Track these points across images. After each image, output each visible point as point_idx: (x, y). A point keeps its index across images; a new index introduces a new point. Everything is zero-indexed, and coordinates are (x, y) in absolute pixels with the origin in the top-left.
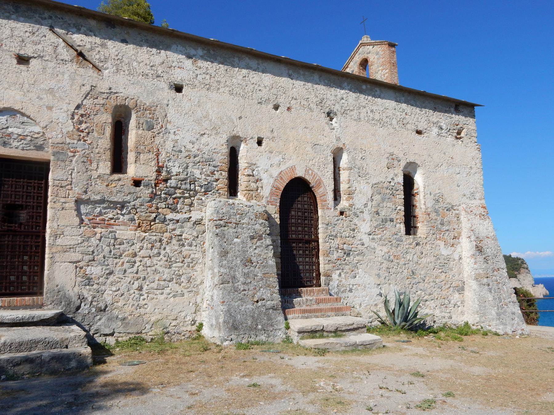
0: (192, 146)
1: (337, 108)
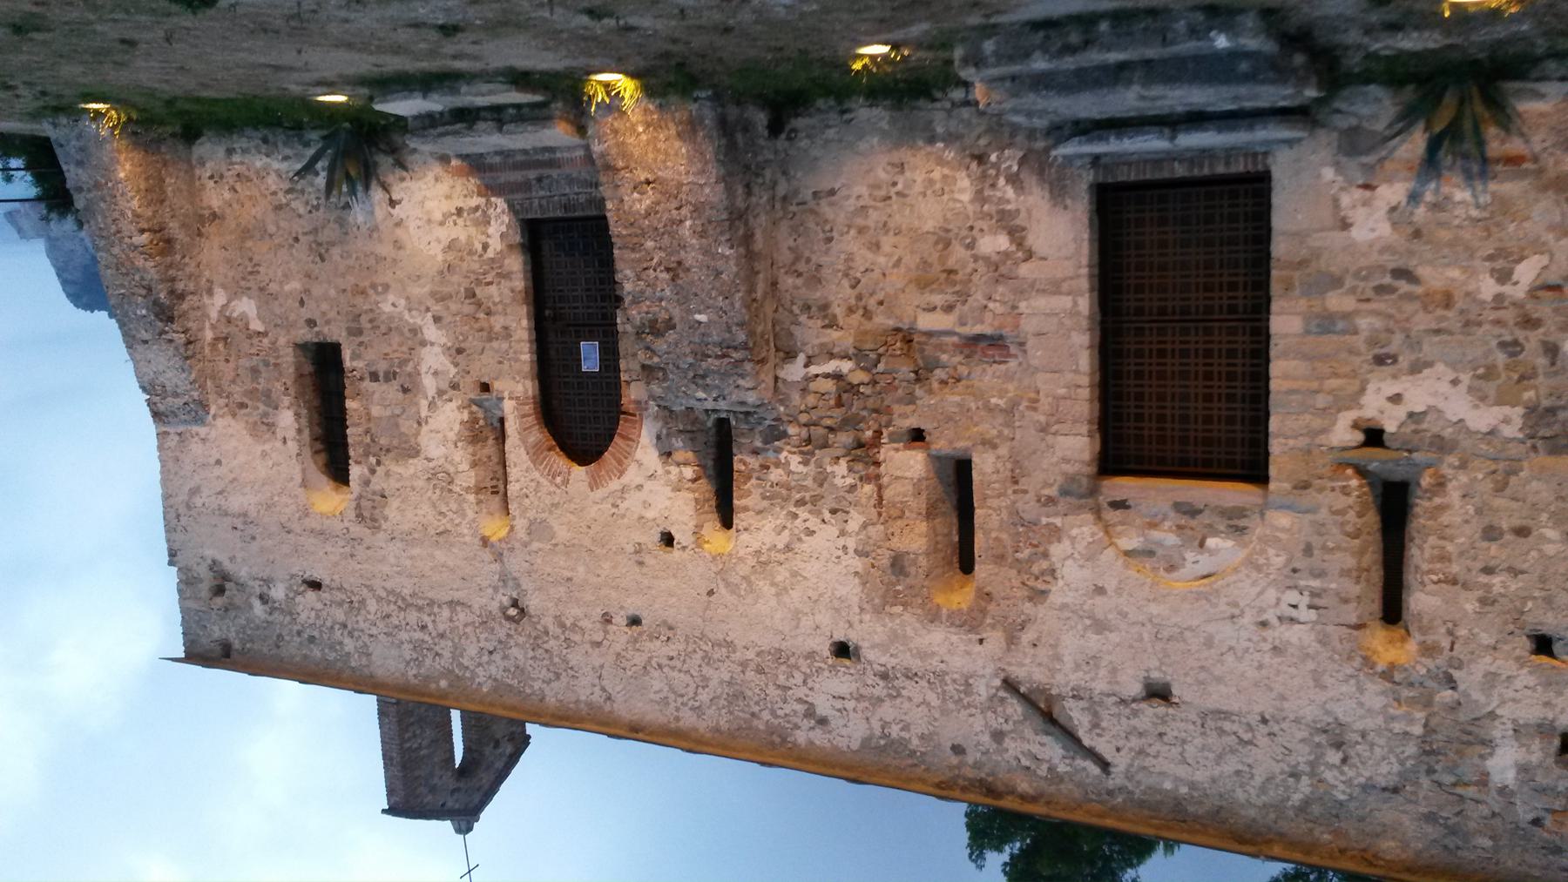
0: (808, 524)
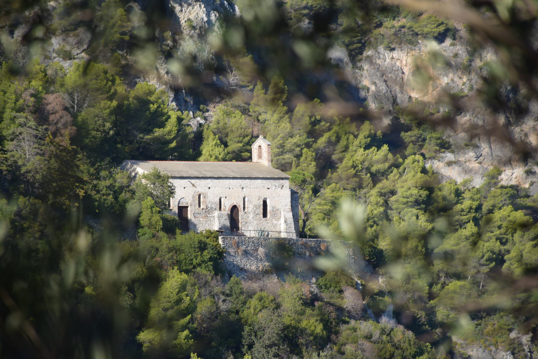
1: (244, 186)
